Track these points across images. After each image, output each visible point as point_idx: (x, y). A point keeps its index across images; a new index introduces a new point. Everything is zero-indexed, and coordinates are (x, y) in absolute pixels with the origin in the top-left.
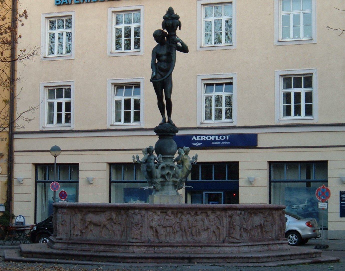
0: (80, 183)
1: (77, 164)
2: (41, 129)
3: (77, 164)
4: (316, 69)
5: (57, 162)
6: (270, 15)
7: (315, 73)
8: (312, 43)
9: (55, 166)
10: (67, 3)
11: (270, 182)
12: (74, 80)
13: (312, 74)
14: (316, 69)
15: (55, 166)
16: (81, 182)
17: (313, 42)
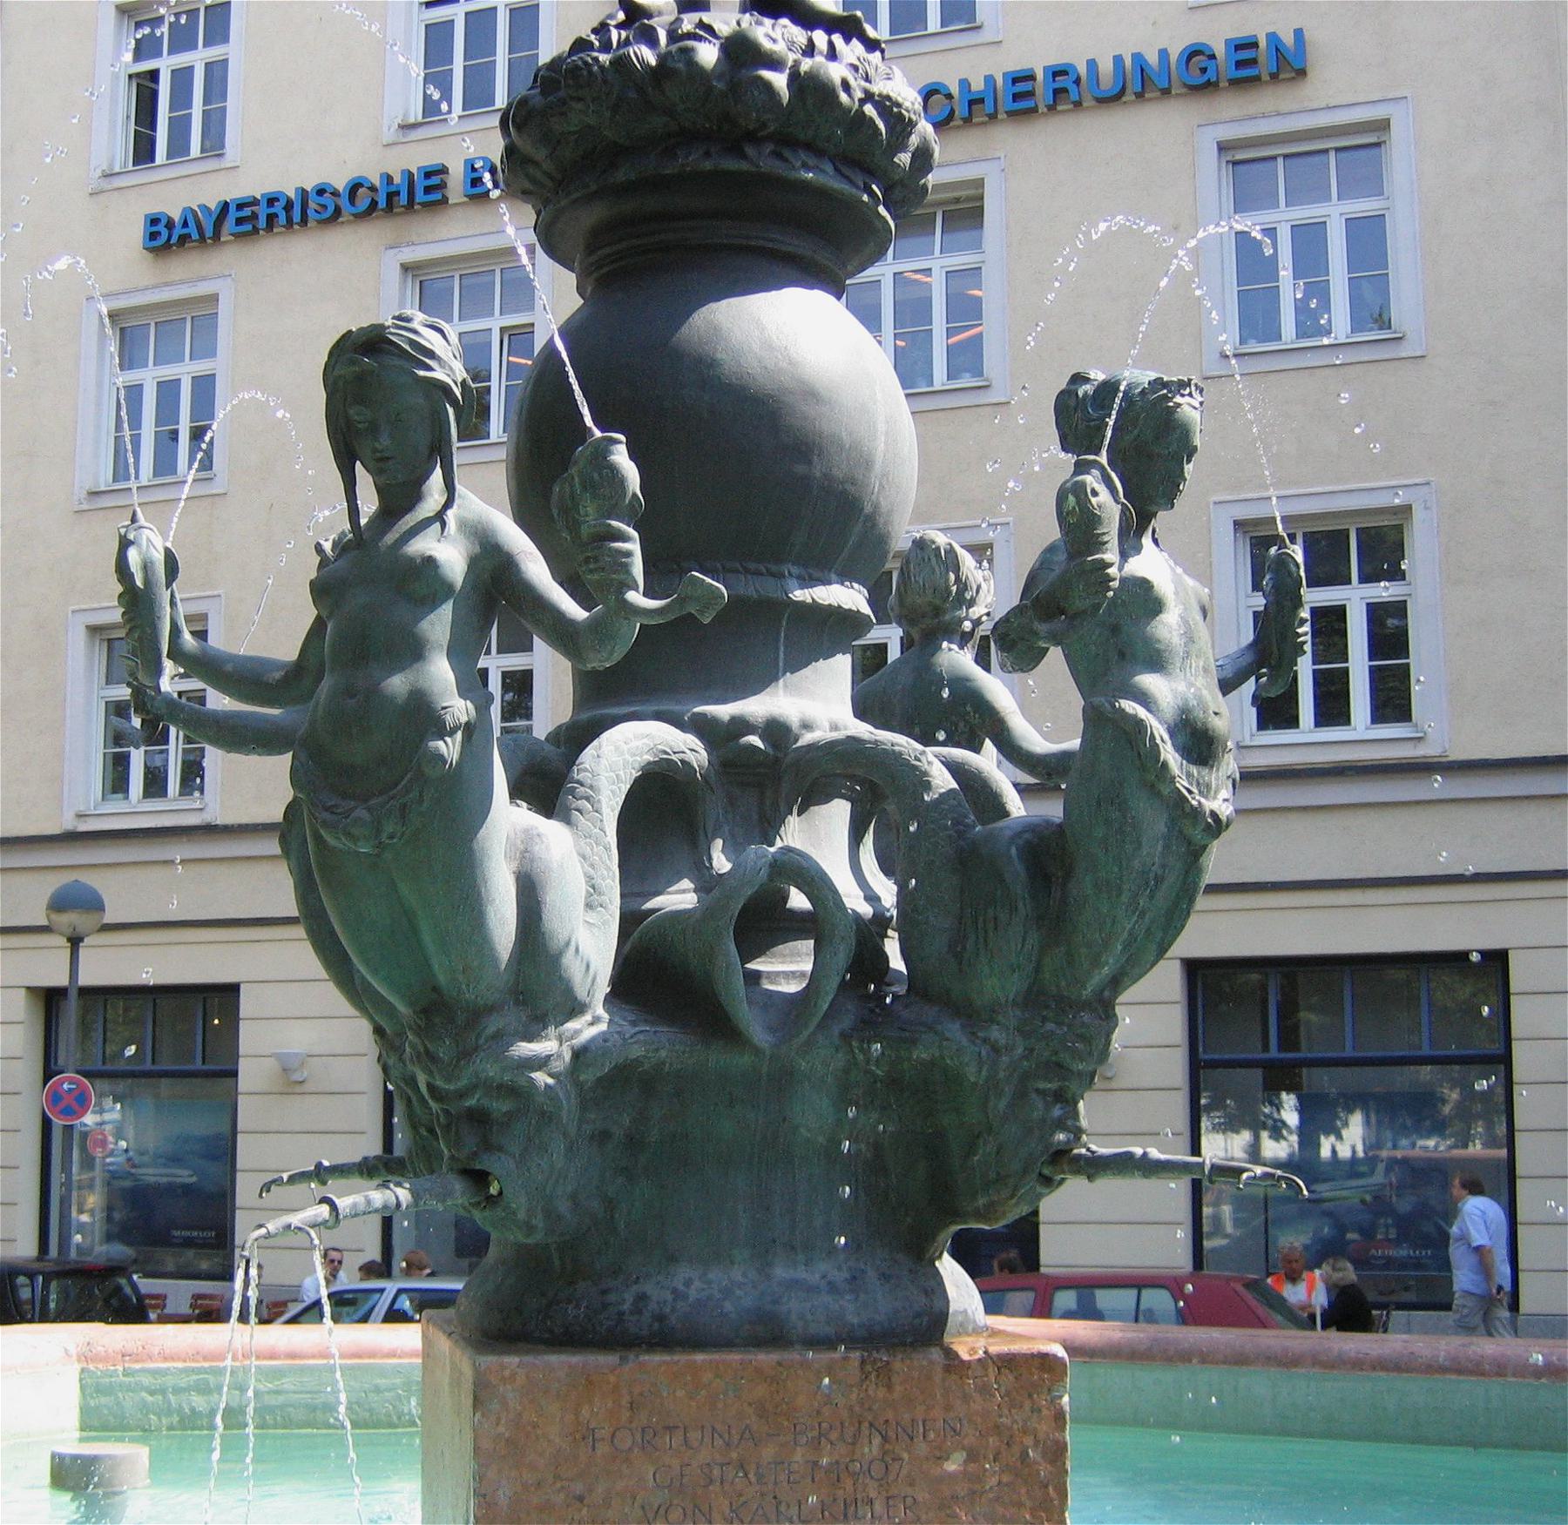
0: (245, 1081)
1: (232, 990)
2: (68, 823)
3: (232, 990)
4: (1428, 484)
5: (85, 979)
6: (1175, 228)
7: (1425, 501)
8: (1404, 355)
9: (73, 994)
10: (195, 236)
11: (1196, 1067)
12: (220, 592)
13: (1406, 510)
14: (1428, 484)
15: (73, 994)
16: (252, 1073)
17: (1405, 351)
